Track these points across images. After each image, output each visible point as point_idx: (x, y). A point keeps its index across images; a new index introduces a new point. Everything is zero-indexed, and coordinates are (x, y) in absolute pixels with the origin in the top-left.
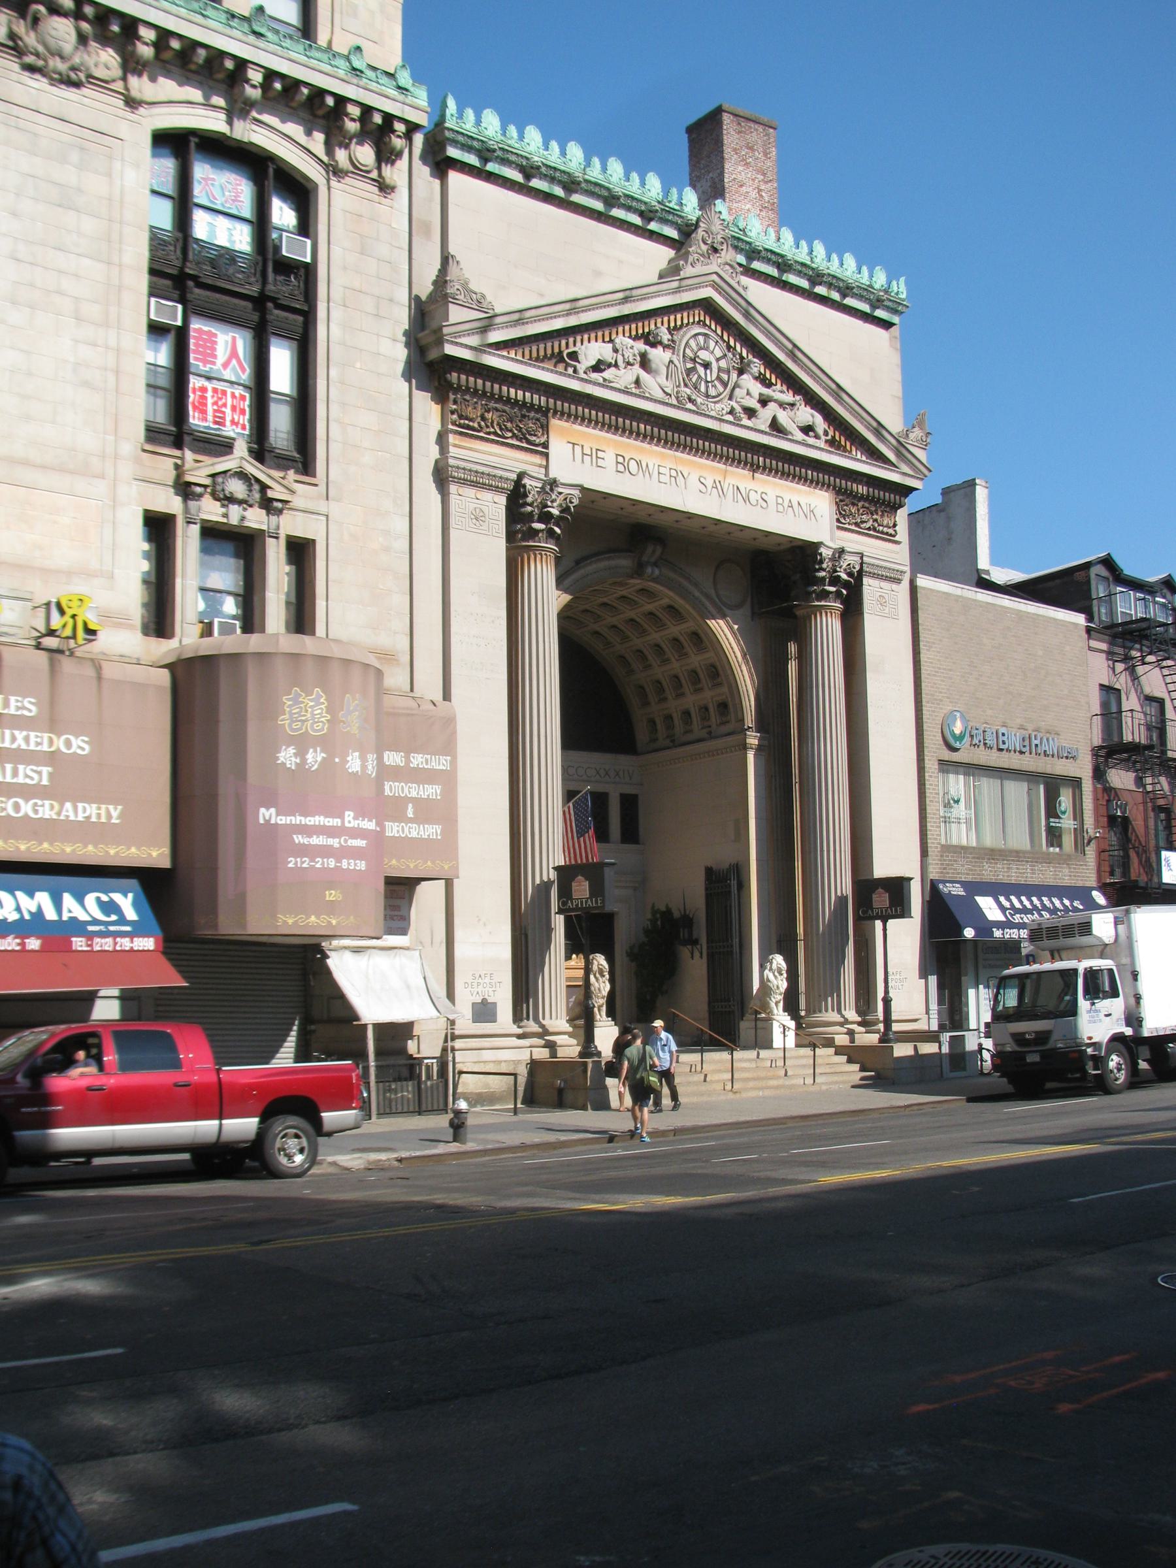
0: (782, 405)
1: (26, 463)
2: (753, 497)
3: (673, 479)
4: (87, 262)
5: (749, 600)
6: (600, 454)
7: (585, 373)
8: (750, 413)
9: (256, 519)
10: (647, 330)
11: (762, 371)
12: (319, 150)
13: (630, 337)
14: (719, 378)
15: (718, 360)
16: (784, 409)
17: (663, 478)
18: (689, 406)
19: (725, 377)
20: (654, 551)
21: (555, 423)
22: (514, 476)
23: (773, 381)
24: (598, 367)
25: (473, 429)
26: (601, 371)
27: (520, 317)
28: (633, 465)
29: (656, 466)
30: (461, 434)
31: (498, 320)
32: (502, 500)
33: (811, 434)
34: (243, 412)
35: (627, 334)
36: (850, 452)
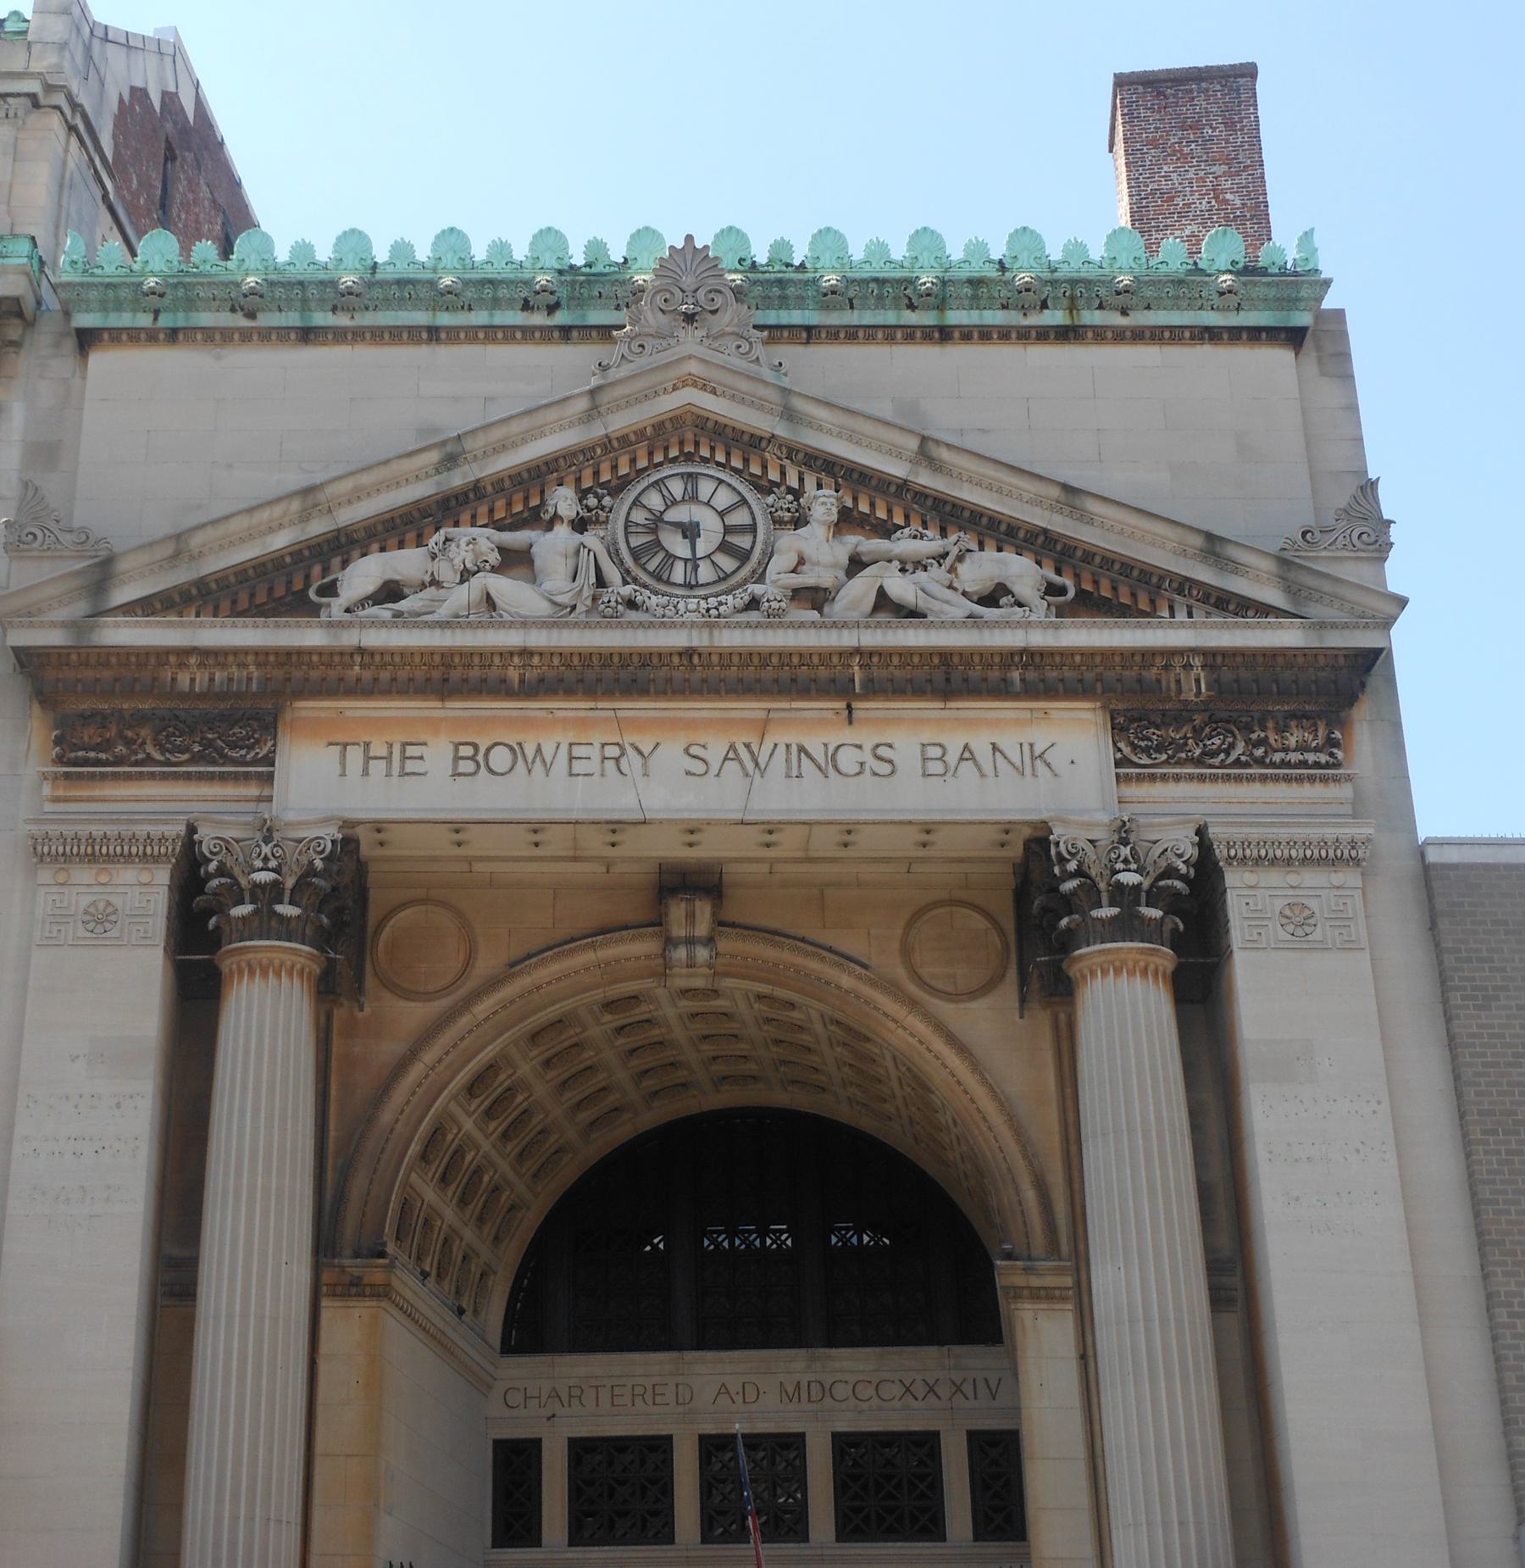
2: (847, 759)
3: (610, 764)
5: (1012, 974)
6: (411, 751)
7: (348, 610)
8: (816, 598)
10: (534, 502)
11: (849, 503)
14: (724, 547)
15: (722, 514)
17: (578, 767)
18: (633, 616)
19: (743, 541)
20: (691, 917)
22: (181, 829)
23: (899, 520)
24: (390, 592)
27: (178, 545)
28: (500, 758)
29: (564, 749)
30: (67, 776)
31: (123, 565)
32: (162, 876)
33: (1003, 601)
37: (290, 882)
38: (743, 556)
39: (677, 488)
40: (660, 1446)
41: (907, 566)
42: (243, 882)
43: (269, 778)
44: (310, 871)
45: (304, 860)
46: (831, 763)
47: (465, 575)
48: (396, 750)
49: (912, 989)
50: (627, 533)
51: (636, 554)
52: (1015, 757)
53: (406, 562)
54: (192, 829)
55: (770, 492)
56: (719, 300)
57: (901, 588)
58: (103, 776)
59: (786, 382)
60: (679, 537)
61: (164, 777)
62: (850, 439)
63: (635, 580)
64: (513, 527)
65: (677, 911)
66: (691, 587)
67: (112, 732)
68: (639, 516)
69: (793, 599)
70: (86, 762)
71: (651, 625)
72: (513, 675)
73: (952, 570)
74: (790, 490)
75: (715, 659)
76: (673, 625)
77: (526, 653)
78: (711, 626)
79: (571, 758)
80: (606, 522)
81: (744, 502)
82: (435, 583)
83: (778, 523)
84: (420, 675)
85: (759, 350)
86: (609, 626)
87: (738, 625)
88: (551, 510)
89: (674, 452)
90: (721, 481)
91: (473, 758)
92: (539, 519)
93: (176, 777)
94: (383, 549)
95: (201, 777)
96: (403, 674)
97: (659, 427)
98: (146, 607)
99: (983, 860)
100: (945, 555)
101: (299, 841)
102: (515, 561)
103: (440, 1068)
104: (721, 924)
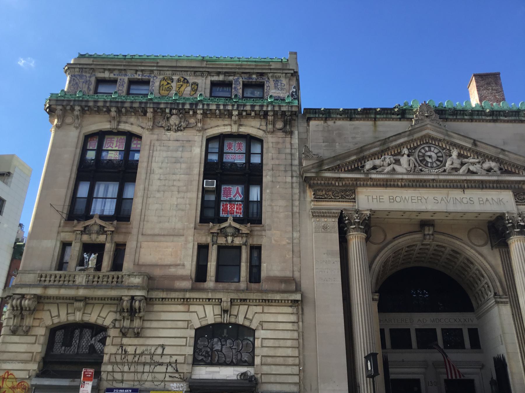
0: (473, 164)
1: (159, 235)
2: (465, 201)
3: (419, 201)
4: (183, 176)
5: (489, 242)
8: (456, 169)
9: (238, 241)
10: (399, 151)
12: (264, 128)
13: (391, 155)
14: (438, 160)
15: (436, 154)
16: (476, 165)
17: (413, 201)
19: (441, 159)
20: (429, 230)
21: (360, 189)
22: (340, 211)
23: (469, 155)
24: (374, 168)
25: (322, 198)
26: (377, 169)
29: (410, 198)
30: (316, 201)
31: (325, 162)
32: (337, 220)
33: (492, 171)
34: (240, 209)
35: (390, 154)
36: (519, 174)
37: (361, 222)
38: (441, 162)
39: (427, 149)
40: (408, 330)
41: (473, 164)
42: (352, 221)
43: (355, 202)
44: (365, 219)
45: (364, 218)
46: (461, 202)
47: (389, 165)
48: (378, 197)
49: (470, 244)
50: (419, 157)
51: (421, 161)
52: (496, 200)
53: (378, 162)
54: (342, 211)
55: (443, 150)
56: (432, 113)
57: (472, 168)
58: (323, 201)
59: (447, 129)
60: (428, 158)
61: (335, 201)
62: (459, 140)
63: (421, 166)
64: (395, 156)
65: (427, 228)
66: (432, 167)
67: (324, 192)
68: (421, 154)
69: (452, 170)
70: (320, 198)
71: (425, 174)
72: (399, 184)
73: (481, 165)
74: (448, 149)
75: (438, 181)
76: (431, 175)
77: (402, 179)
78: (438, 175)
79: (412, 199)
80: (413, 155)
81: (440, 152)
82: (383, 166)
83: (446, 155)
84: (382, 183)
85: (441, 123)
86: (419, 175)
87: (441, 175)
88: (403, 153)
89: (425, 142)
90: (435, 148)
91: (393, 199)
92: (400, 154)
93: (337, 201)
94: (371, 160)
95: (342, 201)
96: (378, 183)
97: (422, 137)
98: (328, 170)
99: (473, 220)
100: (479, 162)
101: (362, 214)
102: (398, 162)
103: (383, 257)
104: (435, 232)
